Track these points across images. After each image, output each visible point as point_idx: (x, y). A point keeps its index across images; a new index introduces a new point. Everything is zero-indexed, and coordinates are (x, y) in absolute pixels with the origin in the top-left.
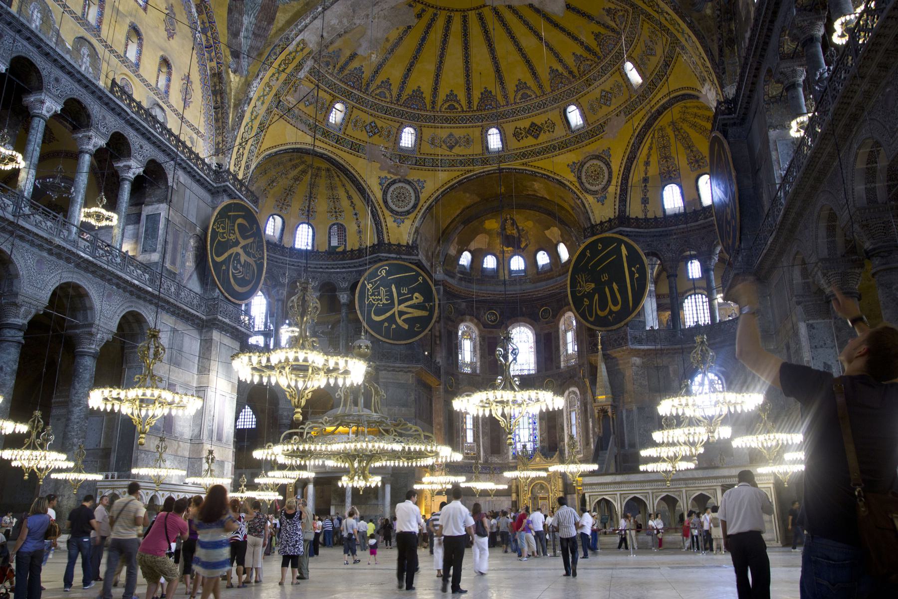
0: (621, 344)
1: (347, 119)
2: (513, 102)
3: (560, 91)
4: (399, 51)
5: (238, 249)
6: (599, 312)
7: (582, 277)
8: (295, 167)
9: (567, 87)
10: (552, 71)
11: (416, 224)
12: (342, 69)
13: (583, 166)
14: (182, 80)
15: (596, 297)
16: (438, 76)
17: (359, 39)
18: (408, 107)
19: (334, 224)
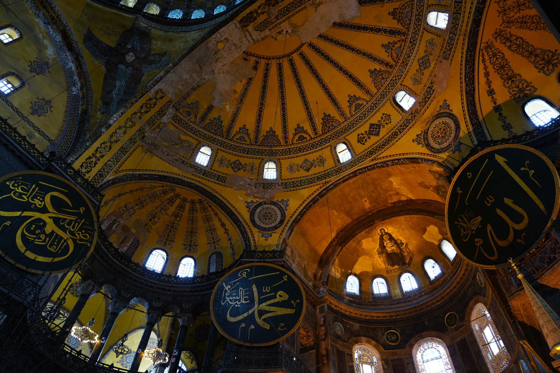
0: (555, 258)
1: (213, 159)
2: (349, 116)
3: (385, 86)
4: (247, 100)
5: (45, 217)
6: (501, 243)
7: (462, 218)
8: (171, 201)
9: (389, 80)
10: (371, 72)
11: (284, 236)
12: (203, 118)
13: (427, 133)
14: (37, 98)
15: (489, 228)
16: (284, 116)
17: (212, 93)
18: (265, 146)
19: (213, 254)
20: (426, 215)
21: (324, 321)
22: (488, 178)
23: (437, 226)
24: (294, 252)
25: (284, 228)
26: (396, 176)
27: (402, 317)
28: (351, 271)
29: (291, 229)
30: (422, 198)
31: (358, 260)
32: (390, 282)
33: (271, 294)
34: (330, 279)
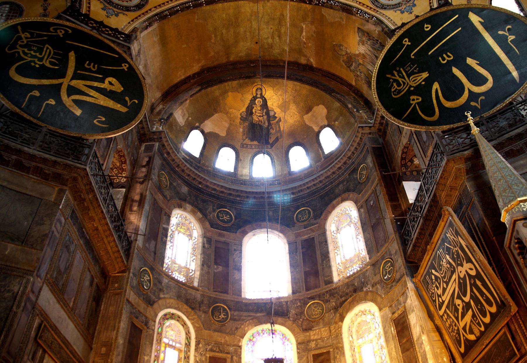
7: (399, 72)
15: (436, 86)
20: (321, 89)
21: (148, 163)
22: (453, 34)
23: (327, 108)
24: (141, 56)
25: (140, 16)
26: (312, 23)
27: (242, 199)
28: (200, 125)
29: (150, 22)
30: (326, 68)
31: (213, 115)
32: (241, 157)
33: (98, 76)
34: (171, 119)
